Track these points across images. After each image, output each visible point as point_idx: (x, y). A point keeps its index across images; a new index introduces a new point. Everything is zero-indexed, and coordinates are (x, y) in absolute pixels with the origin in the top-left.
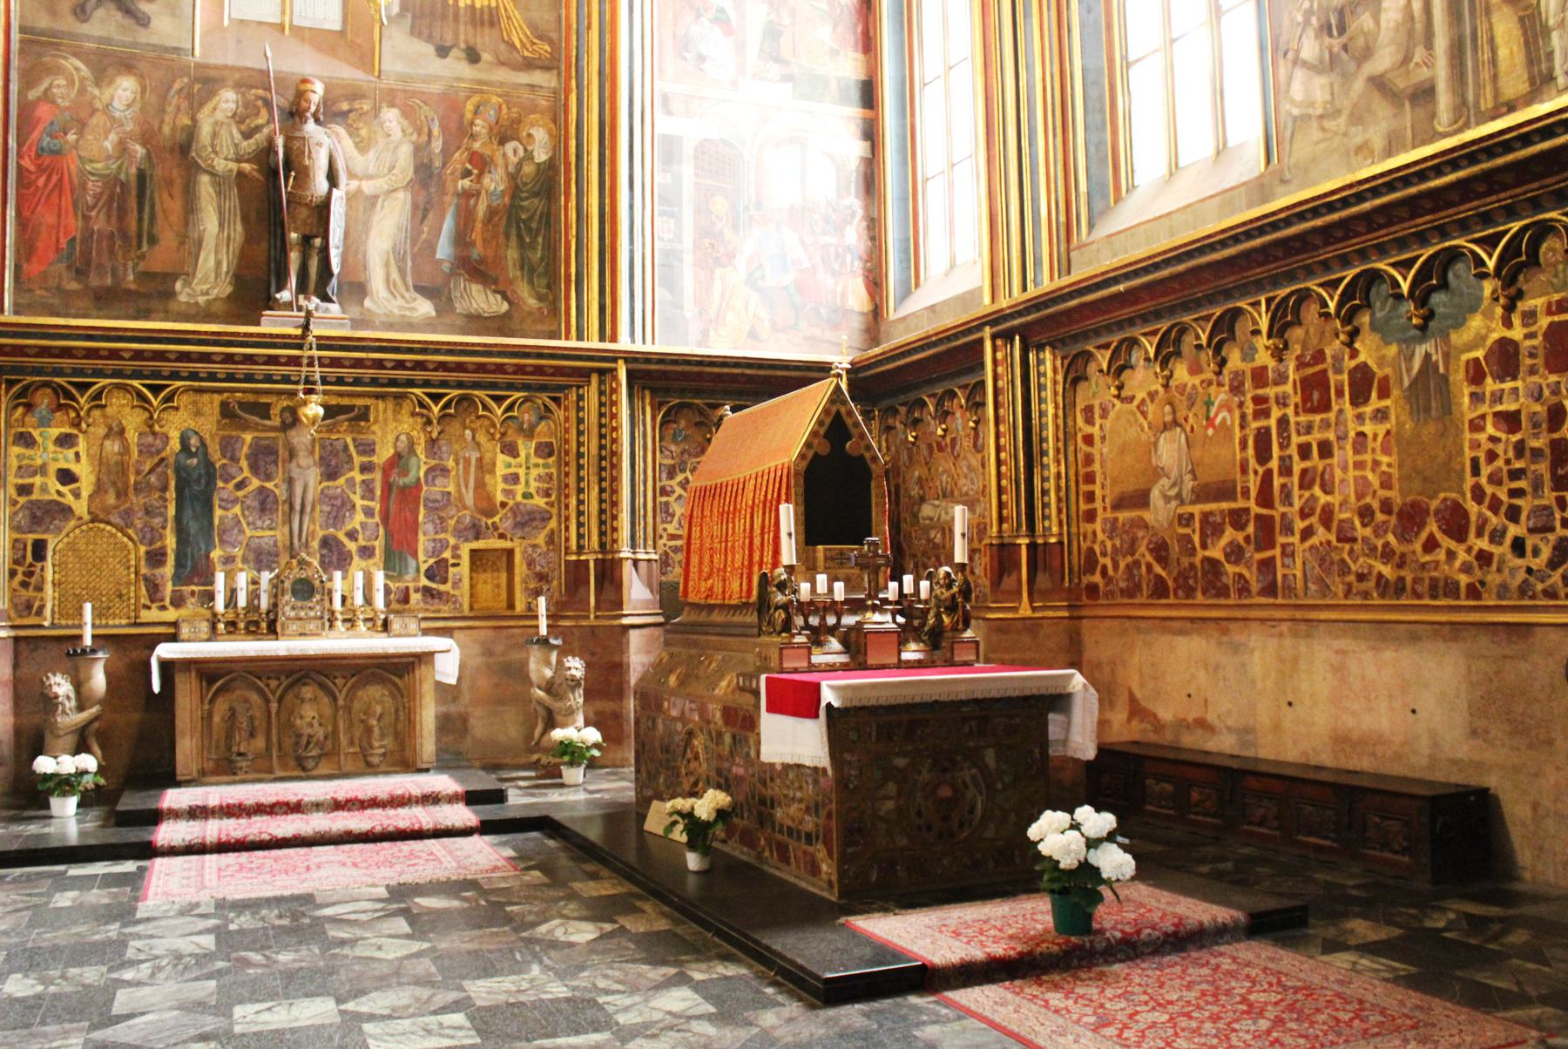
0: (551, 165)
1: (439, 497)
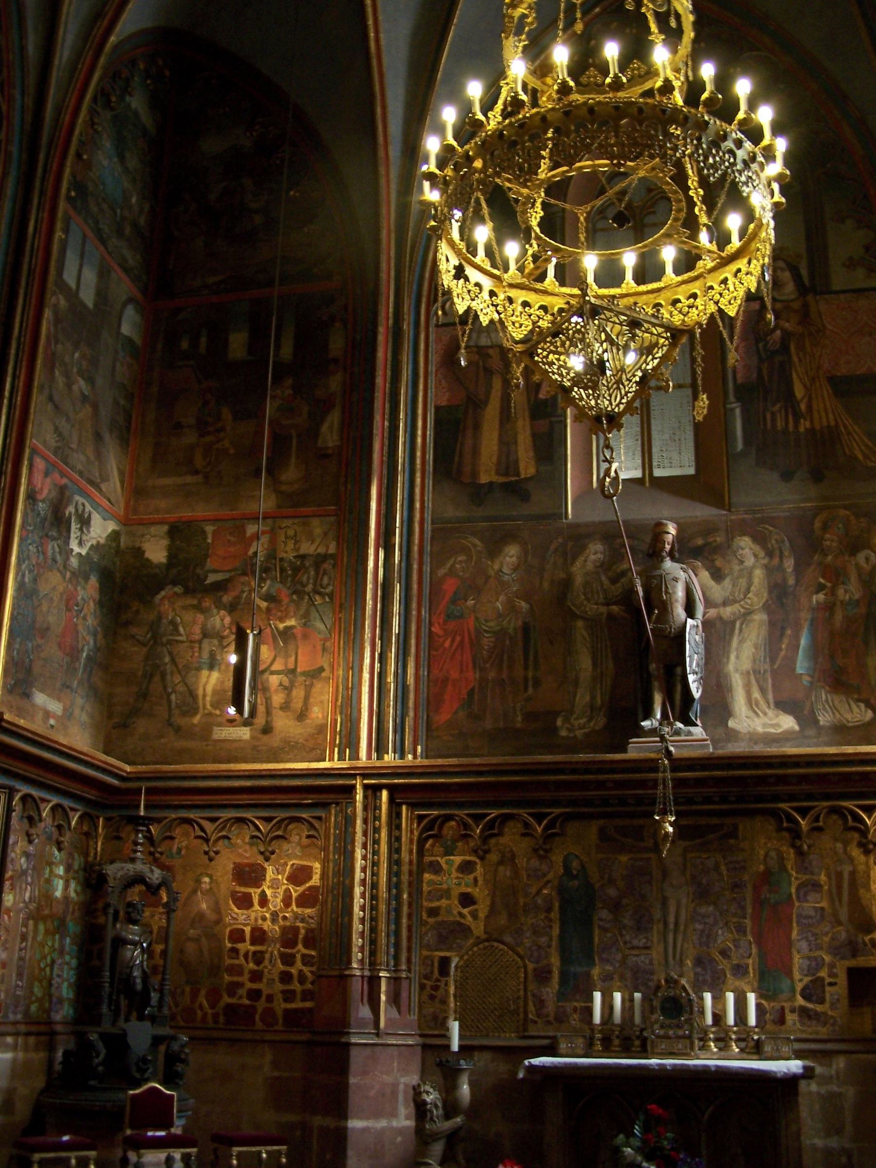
1: (812, 913)
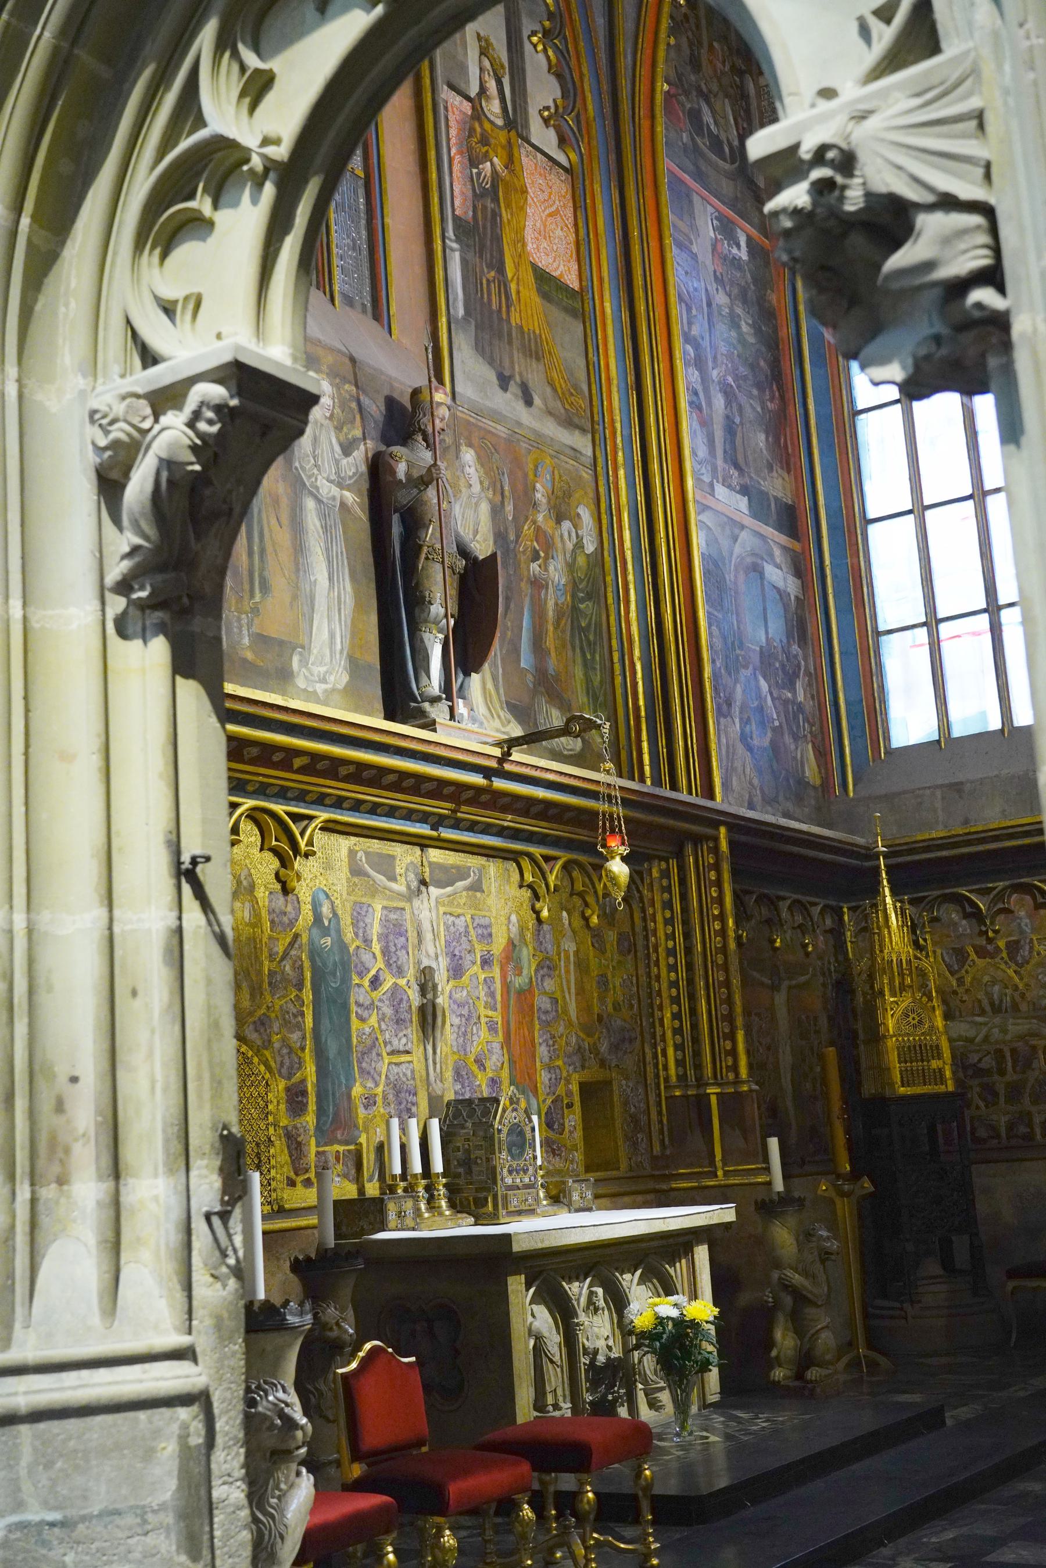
0: (597, 560)
